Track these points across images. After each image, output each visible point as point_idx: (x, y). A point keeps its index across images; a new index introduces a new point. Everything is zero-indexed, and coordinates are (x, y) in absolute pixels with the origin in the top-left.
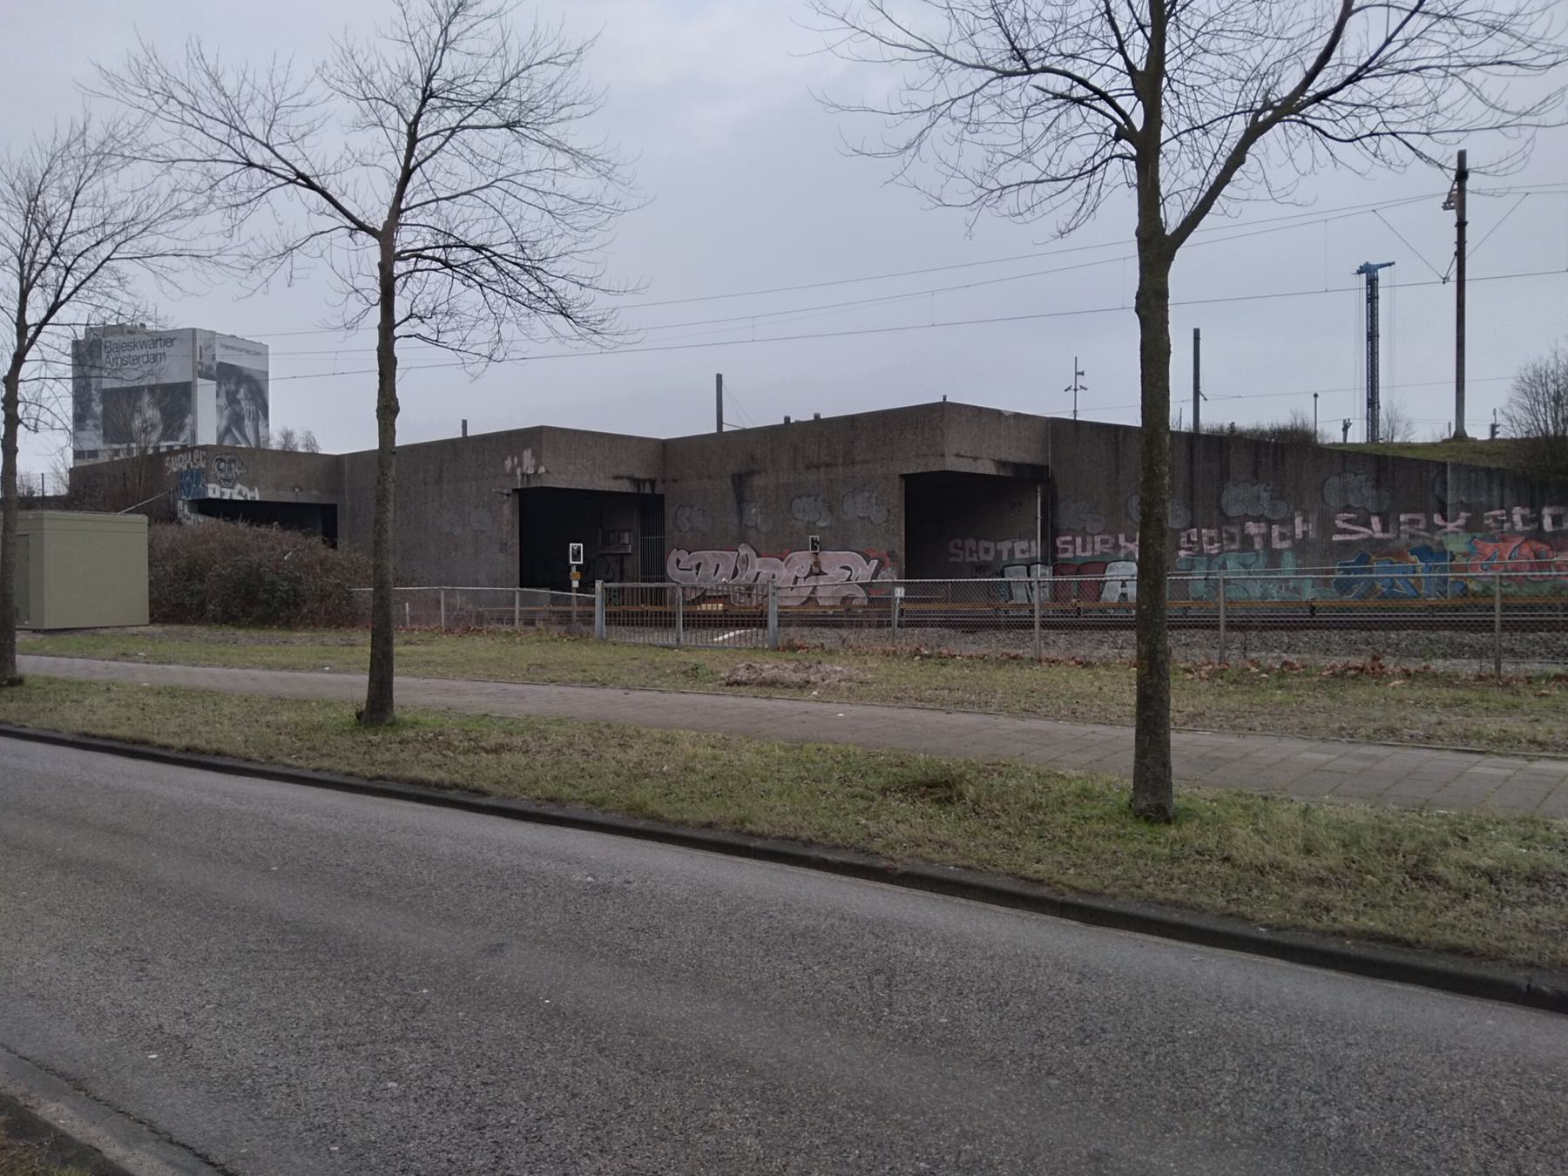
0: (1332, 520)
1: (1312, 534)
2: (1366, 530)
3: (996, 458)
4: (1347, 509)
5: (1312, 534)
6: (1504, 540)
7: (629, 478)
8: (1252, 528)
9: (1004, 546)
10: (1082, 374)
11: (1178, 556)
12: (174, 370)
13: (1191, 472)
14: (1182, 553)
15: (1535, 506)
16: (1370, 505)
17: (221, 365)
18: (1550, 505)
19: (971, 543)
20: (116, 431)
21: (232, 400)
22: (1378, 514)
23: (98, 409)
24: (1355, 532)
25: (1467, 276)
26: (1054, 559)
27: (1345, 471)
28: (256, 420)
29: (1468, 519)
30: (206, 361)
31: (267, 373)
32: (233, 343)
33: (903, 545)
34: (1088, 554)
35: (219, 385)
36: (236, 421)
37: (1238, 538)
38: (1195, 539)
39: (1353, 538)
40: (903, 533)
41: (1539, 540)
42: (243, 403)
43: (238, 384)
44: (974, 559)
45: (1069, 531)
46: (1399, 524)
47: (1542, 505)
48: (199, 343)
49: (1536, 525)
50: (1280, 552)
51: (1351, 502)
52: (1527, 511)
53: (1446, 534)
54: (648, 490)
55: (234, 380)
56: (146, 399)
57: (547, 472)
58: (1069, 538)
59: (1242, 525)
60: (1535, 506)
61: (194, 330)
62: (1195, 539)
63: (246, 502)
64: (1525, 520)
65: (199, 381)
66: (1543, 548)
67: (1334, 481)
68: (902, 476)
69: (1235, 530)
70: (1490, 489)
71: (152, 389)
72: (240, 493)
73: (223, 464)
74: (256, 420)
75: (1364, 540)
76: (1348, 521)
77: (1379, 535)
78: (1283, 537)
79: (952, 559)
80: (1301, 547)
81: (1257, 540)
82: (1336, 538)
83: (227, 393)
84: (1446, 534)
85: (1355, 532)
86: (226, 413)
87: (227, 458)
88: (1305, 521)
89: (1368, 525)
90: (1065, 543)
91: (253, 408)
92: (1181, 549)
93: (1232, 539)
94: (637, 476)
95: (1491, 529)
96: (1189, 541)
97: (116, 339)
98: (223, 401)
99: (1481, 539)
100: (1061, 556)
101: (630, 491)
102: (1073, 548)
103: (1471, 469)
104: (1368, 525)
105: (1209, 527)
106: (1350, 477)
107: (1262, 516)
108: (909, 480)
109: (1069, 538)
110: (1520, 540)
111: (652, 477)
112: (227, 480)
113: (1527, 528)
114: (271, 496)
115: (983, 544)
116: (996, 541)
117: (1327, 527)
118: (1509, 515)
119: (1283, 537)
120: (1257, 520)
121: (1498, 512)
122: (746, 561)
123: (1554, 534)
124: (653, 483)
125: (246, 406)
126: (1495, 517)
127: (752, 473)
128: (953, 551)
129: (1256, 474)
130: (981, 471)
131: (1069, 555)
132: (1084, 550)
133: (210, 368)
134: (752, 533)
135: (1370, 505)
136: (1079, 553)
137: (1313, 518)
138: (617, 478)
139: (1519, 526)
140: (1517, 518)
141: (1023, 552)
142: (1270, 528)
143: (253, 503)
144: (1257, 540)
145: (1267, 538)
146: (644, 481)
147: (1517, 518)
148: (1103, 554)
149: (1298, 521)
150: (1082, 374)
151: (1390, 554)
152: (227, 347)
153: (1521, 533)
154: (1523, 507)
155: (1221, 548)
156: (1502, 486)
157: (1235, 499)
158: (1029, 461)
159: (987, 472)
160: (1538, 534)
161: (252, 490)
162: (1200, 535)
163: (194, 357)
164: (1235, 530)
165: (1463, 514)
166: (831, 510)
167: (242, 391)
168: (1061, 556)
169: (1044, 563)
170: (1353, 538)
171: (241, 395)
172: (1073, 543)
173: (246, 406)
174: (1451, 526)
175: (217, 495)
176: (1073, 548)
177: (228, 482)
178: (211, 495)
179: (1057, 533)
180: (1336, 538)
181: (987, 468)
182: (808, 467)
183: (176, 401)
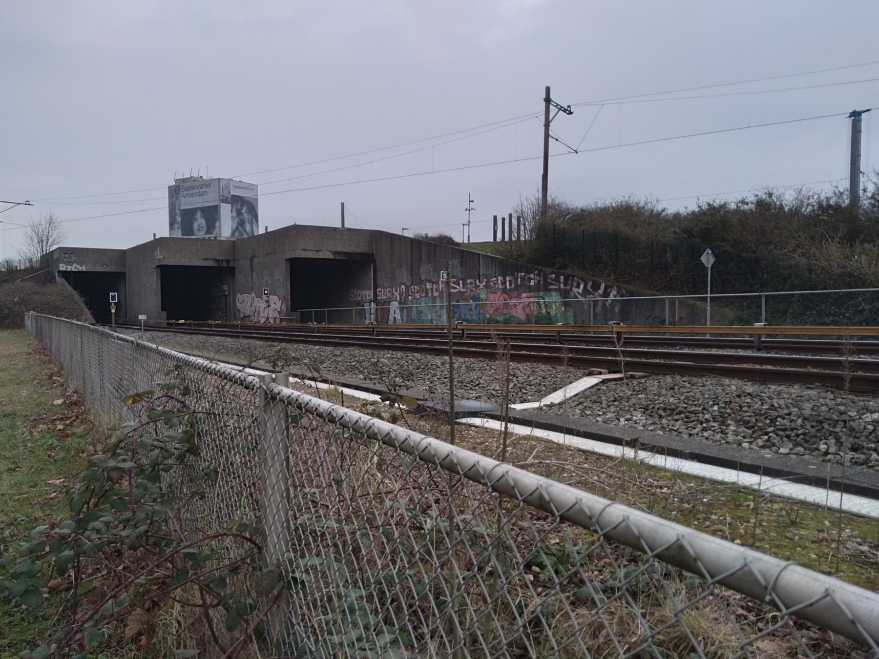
7: (212, 259)
8: (429, 286)
9: (364, 292)
10: (473, 201)
12: (209, 200)
16: (459, 275)
17: (233, 196)
19: (355, 291)
20: (187, 228)
21: (239, 213)
22: (462, 279)
23: (179, 219)
24: (456, 288)
26: (377, 300)
28: (251, 224)
30: (226, 194)
31: (257, 199)
32: (241, 185)
34: (385, 297)
35: (232, 206)
36: (242, 223)
40: (289, 287)
42: (245, 215)
43: (242, 205)
44: (355, 299)
48: (222, 185)
54: (225, 264)
55: (239, 204)
56: (199, 214)
58: (380, 289)
61: (219, 179)
63: (78, 272)
65: (222, 204)
68: (287, 259)
69: (423, 287)
71: (203, 209)
72: (76, 268)
73: (66, 256)
74: (251, 224)
76: (454, 283)
77: (462, 290)
81: (430, 291)
82: (452, 291)
83: (237, 210)
85: (456, 288)
86: (236, 220)
87: (69, 252)
89: (459, 285)
91: (250, 217)
94: (218, 258)
97: (186, 185)
98: (234, 214)
100: (379, 298)
103: (487, 257)
104: (459, 285)
109: (380, 289)
111: (228, 258)
112: (69, 262)
114: (91, 269)
115: (359, 292)
118: (497, 280)
120: (430, 281)
121: (494, 279)
122: (253, 299)
124: (228, 261)
125: (246, 216)
127: (254, 257)
133: (227, 198)
138: (205, 259)
139: (500, 287)
140: (499, 282)
143: (82, 272)
144: (430, 291)
145: (432, 289)
146: (222, 261)
147: (499, 282)
150: (473, 201)
152: (236, 187)
153: (500, 289)
157: (425, 270)
158: (357, 250)
160: (505, 290)
161: (81, 266)
163: (219, 191)
165: (485, 280)
166: (271, 276)
167: (244, 209)
168: (379, 298)
171: (244, 211)
173: (246, 216)
174: (481, 285)
175: (64, 269)
177: (70, 263)
178: (61, 269)
179: (377, 288)
183: (211, 214)
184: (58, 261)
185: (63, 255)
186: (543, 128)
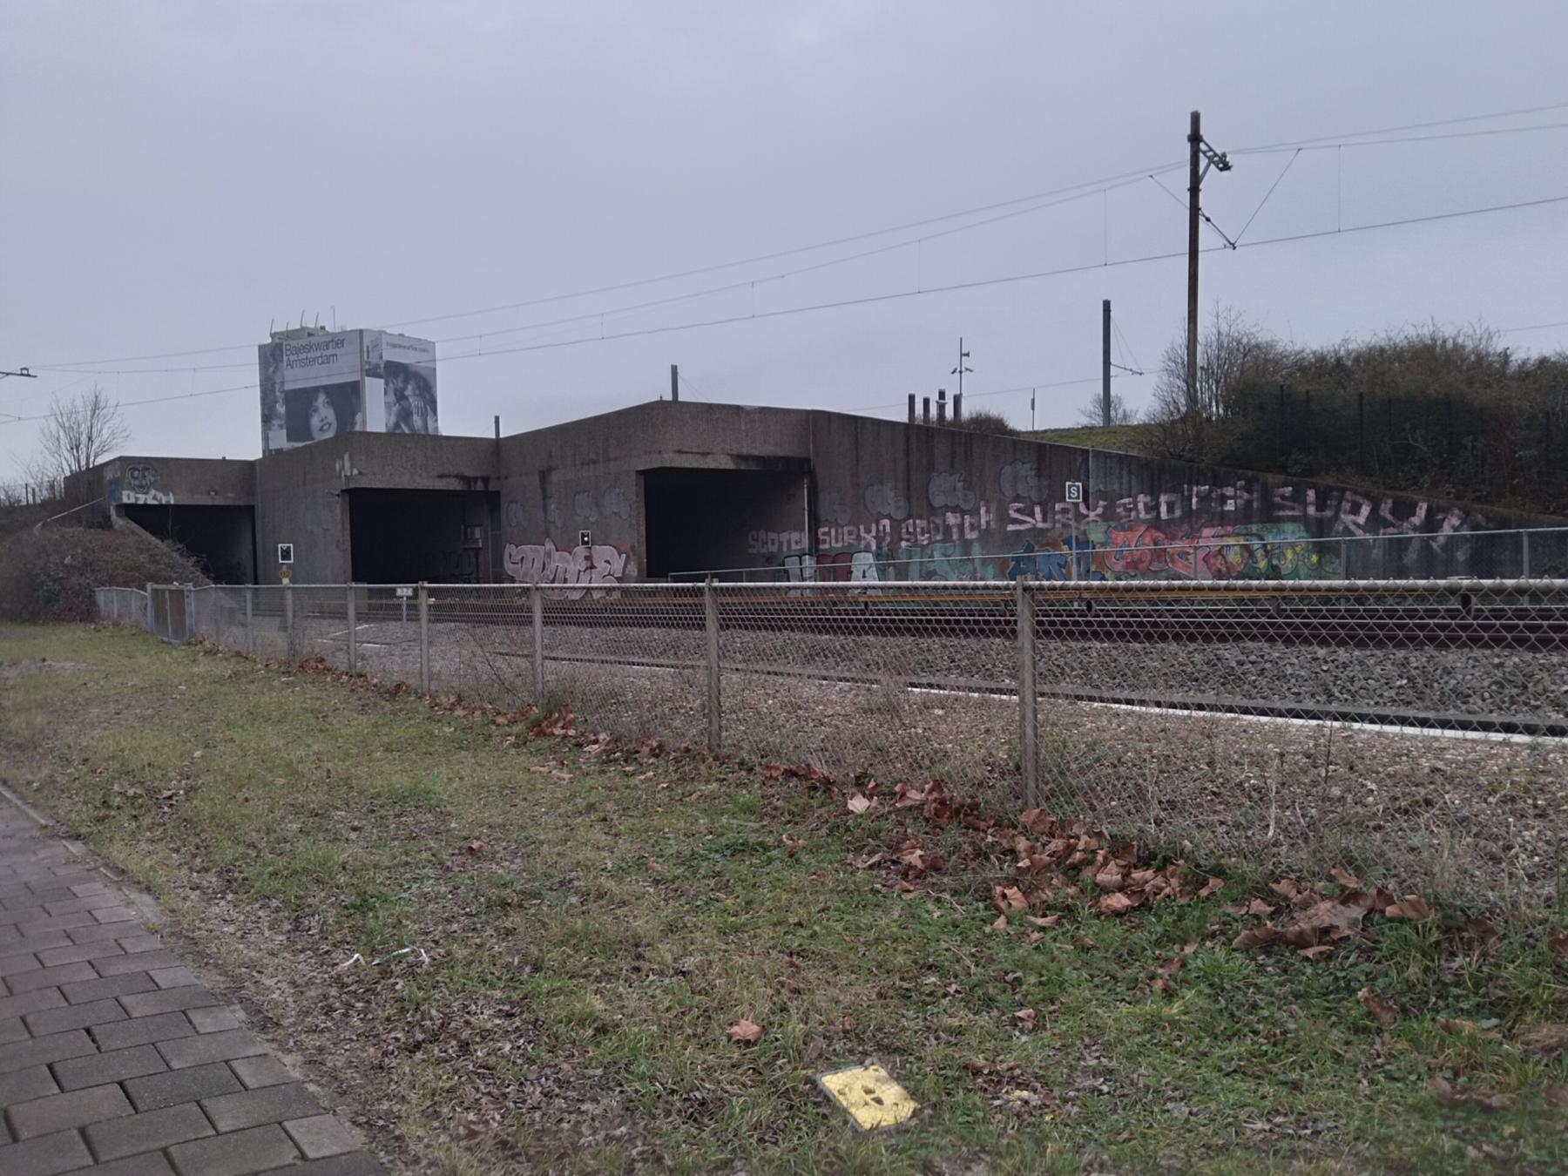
0: (1007, 510)
1: (993, 525)
2: (1028, 519)
3: (734, 452)
4: (1017, 498)
5: (993, 525)
6: (1131, 529)
7: (456, 476)
8: (952, 519)
9: (784, 537)
11: (900, 547)
12: (341, 372)
13: (908, 463)
14: (904, 544)
15: (1154, 493)
16: (1034, 495)
17: (389, 364)
18: (1166, 492)
19: (762, 534)
20: (298, 425)
21: (400, 396)
22: (1039, 503)
23: (281, 409)
24: (1023, 522)
25: (1201, 247)
26: (817, 550)
27: (1015, 460)
28: (424, 416)
29: (1105, 507)
30: (374, 359)
31: (434, 370)
32: (401, 343)
33: (644, 539)
34: (839, 545)
35: (387, 384)
36: (405, 415)
37: (941, 528)
38: (911, 530)
39: (1022, 527)
40: (643, 528)
41: (1158, 529)
42: (411, 400)
43: (406, 382)
44: (764, 550)
45: (828, 523)
46: (1055, 513)
47: (1160, 492)
48: (366, 342)
49: (1155, 513)
50: (971, 541)
51: (1020, 492)
52: (1148, 499)
53: (1088, 523)
54: (480, 486)
55: (400, 379)
56: (322, 398)
57: (360, 473)
58: (826, 529)
59: (944, 515)
60: (1154, 493)
61: (361, 332)
62: (911, 530)
63: (161, 506)
64: (1148, 509)
65: (367, 380)
66: (1161, 536)
67: (1008, 469)
68: (639, 472)
69: (938, 521)
70: (1121, 477)
71: (328, 390)
72: (155, 498)
73: (136, 473)
74: (424, 416)
75: (1029, 530)
76: (1018, 511)
77: (1040, 525)
78: (972, 527)
79: (751, 551)
80: (985, 535)
81: (955, 530)
82: (1011, 528)
83: (396, 391)
84: (1088, 523)
85: (1023, 522)
86: (394, 410)
87: (140, 467)
88: (988, 511)
89: (1032, 515)
90: (824, 534)
91: (421, 404)
92: (901, 539)
93: (937, 529)
94: (466, 474)
95: (1121, 518)
96: (908, 533)
97: (293, 343)
98: (391, 398)
99: (1115, 528)
100: (822, 547)
101: (458, 488)
102: (832, 540)
103: (1108, 456)
104: (1032, 515)
105: (921, 518)
106: (1019, 465)
107: (957, 506)
108: (645, 474)
109: (826, 529)
110: (1143, 529)
111: (485, 474)
112: (141, 487)
113: (1149, 516)
114: (186, 500)
115: (772, 535)
116: (780, 532)
117: (1004, 518)
118: (1135, 503)
119: (972, 527)
120: (954, 510)
121: (1126, 500)
122: (549, 555)
123: (1169, 521)
124: (486, 480)
125: (414, 402)
126: (1124, 505)
127: (551, 469)
128: (752, 543)
129: (952, 465)
130: (713, 466)
131: (826, 546)
132: (837, 541)
133: (377, 366)
134: (553, 529)
135: (1034, 495)
136: (834, 545)
137: (993, 507)
138: (441, 477)
139: (1143, 515)
140: (1141, 506)
141: (797, 543)
142: (963, 519)
143: (167, 507)
144: (955, 530)
145: (961, 527)
146: (476, 479)
147: (1141, 506)
148: (850, 545)
149: (983, 510)
151: (1047, 544)
152: (394, 346)
153: (1144, 521)
154: (1146, 495)
155: (929, 538)
156: (1130, 473)
157: (943, 487)
158: (780, 452)
159: (723, 467)
160: (1156, 524)
161: (166, 494)
162: (915, 526)
163: (362, 357)
164: (938, 521)
165: (1102, 503)
166: (597, 506)
167: (410, 387)
168: (822, 547)
169: (810, 555)
170: (1022, 527)
171: (408, 392)
172: (829, 534)
173: (414, 402)
174: (1092, 515)
175: (132, 501)
176: (832, 540)
177: (144, 489)
178: (125, 500)
179: (818, 527)
180: (1011, 528)
181: (727, 464)
182: (583, 464)
183: (347, 398)
184: (117, 484)
185: (128, 474)
186: (1188, 194)
